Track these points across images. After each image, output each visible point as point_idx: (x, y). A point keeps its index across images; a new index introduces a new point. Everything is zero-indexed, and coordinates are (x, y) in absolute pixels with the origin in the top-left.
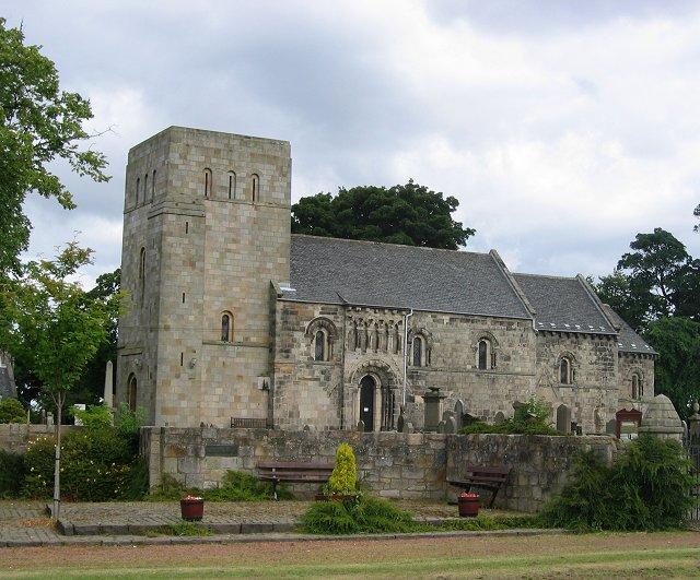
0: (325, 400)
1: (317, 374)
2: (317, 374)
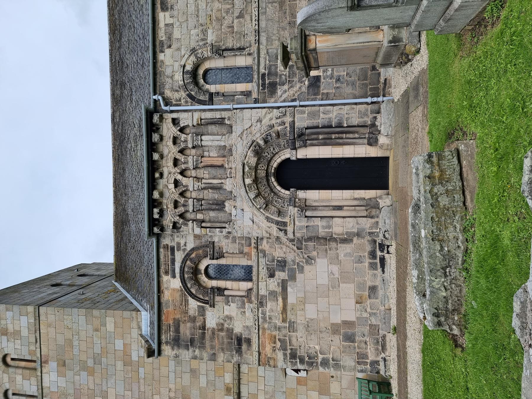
0: (321, 270)
1: (273, 284)
2: (273, 284)
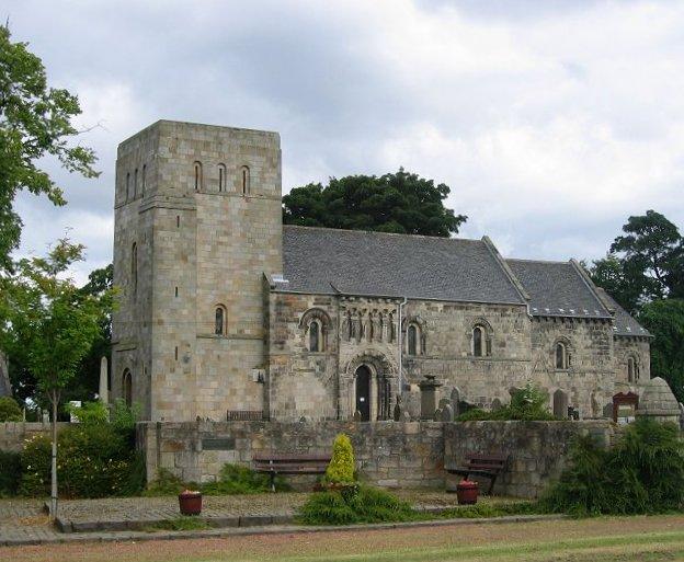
0: (320, 391)
1: (312, 365)
2: (312, 365)
